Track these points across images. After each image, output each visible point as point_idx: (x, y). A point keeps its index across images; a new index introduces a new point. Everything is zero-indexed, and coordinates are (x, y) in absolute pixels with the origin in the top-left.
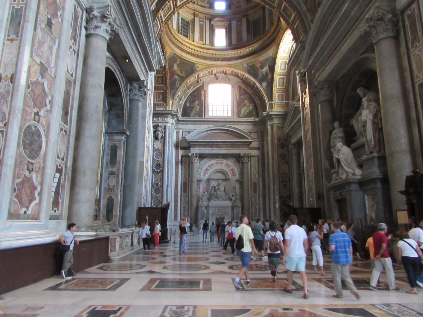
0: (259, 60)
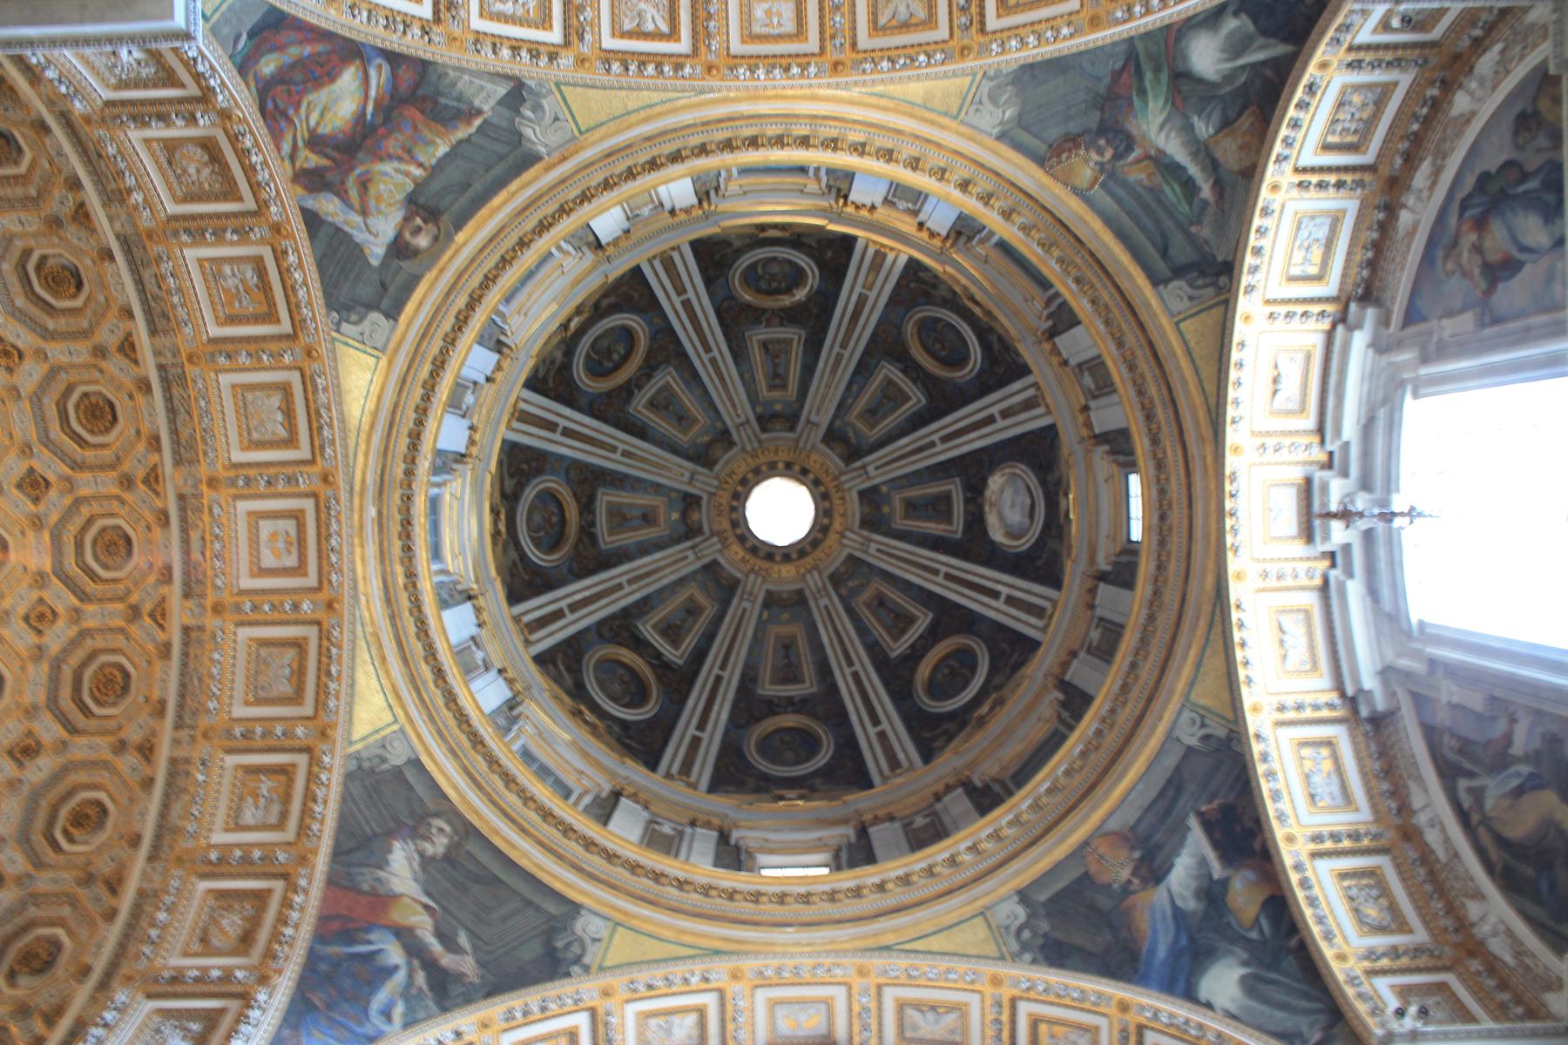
0: (1114, 824)
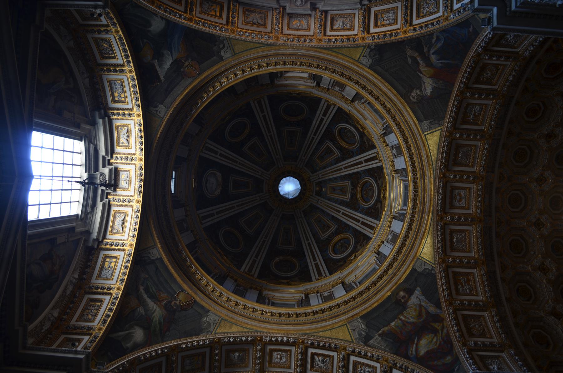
0: (189, 80)
